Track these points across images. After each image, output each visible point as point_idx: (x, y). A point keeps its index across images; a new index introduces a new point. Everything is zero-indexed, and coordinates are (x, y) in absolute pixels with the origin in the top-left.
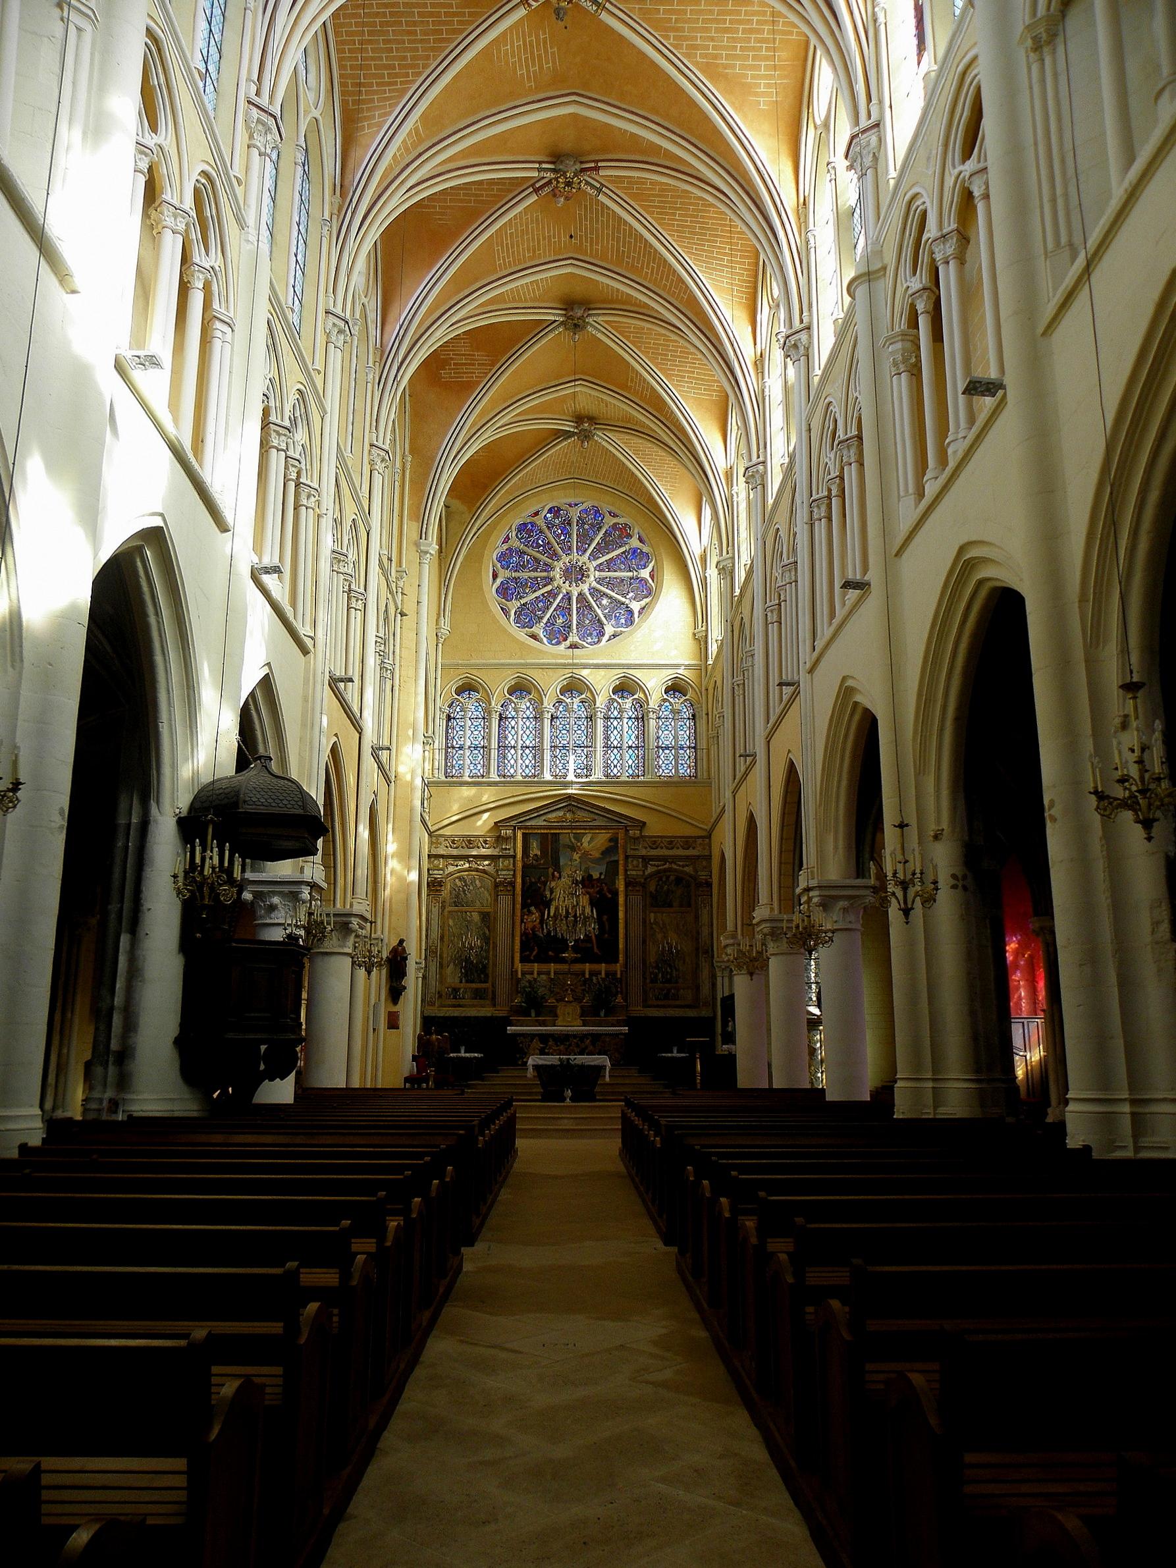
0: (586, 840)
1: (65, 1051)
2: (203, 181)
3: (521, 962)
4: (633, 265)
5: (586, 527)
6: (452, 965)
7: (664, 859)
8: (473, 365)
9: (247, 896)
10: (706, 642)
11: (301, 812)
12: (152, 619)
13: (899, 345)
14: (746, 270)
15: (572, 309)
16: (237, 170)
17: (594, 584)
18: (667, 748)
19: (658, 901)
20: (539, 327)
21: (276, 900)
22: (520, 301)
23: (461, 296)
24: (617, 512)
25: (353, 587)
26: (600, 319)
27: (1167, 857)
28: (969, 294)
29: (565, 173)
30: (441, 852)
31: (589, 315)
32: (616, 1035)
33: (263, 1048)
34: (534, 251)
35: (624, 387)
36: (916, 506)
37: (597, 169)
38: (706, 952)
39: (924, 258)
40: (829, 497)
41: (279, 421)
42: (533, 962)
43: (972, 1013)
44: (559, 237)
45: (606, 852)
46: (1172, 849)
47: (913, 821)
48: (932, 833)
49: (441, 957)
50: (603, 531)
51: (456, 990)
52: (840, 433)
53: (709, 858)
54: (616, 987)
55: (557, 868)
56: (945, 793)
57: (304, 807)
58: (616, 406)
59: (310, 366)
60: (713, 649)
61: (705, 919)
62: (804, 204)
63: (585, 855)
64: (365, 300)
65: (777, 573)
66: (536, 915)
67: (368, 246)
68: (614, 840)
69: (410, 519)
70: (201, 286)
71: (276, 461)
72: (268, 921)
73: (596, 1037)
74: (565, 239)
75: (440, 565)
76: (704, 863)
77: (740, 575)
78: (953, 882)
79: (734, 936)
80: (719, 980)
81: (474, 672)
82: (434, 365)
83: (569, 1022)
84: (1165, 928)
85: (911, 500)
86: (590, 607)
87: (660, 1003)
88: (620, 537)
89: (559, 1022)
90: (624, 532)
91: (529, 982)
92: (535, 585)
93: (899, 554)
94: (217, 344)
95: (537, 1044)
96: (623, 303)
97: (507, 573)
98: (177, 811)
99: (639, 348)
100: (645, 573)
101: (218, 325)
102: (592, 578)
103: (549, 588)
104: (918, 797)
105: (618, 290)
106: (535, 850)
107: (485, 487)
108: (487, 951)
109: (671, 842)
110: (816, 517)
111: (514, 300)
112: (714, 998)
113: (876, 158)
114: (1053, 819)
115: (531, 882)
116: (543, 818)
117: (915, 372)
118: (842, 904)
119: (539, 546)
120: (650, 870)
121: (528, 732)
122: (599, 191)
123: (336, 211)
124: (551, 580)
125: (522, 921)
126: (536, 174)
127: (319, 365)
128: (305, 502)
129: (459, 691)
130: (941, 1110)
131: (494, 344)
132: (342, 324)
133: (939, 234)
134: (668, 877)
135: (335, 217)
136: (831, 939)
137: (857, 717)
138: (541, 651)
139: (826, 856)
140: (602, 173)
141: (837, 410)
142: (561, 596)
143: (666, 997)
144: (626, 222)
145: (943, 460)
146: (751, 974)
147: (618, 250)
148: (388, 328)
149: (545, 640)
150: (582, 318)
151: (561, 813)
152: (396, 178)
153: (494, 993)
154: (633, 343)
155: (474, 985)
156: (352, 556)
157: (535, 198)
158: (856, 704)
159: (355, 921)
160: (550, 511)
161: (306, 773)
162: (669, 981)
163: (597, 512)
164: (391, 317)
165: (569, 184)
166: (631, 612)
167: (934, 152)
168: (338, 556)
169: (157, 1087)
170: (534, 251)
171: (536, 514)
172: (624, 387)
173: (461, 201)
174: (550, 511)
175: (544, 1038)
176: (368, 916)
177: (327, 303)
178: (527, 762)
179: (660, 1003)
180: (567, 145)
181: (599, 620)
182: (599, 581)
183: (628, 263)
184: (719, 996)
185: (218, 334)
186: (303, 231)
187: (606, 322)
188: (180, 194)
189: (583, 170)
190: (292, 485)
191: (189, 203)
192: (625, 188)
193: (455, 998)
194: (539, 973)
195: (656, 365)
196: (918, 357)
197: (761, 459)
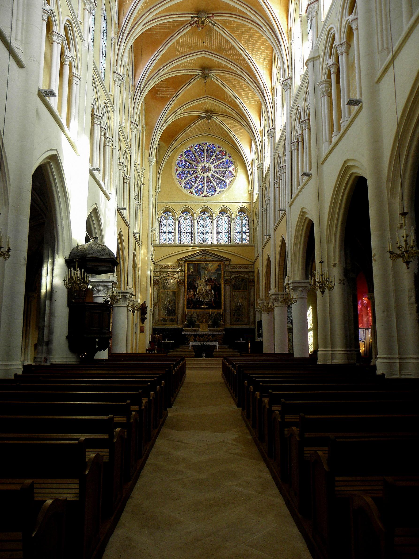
0: (210, 266)
1: (27, 340)
2: (68, 23)
3: (187, 309)
4: (227, 53)
5: (210, 152)
6: (162, 310)
7: (238, 273)
8: (168, 91)
9: (90, 286)
10: (253, 194)
11: (108, 257)
12: (54, 188)
13: (324, 85)
14: (268, 55)
15: (204, 70)
16: (80, 19)
17: (213, 173)
18: (239, 233)
19: (235, 287)
20: (192, 77)
21: (100, 288)
22: (185, 67)
23: (163, 65)
24: (221, 146)
25: (125, 175)
26: (215, 74)
27: (415, 274)
28: (350, 66)
29: (201, 18)
30: (158, 270)
31: (210, 72)
32: (221, 334)
33: (97, 340)
34: (190, 48)
35: (224, 100)
36: (329, 146)
37: (213, 16)
38: (252, 305)
39: (334, 52)
40: (298, 142)
41: (97, 114)
42: (191, 309)
43: (345, 328)
44: (199, 43)
45: (217, 270)
46: (416, 271)
47: (326, 260)
48: (332, 265)
49: (159, 307)
50: (216, 154)
51: (164, 319)
52: (302, 118)
53: (254, 272)
54: (221, 318)
55: (199, 275)
56: (337, 250)
57: (110, 255)
58: (220, 106)
59: (108, 92)
60: (255, 197)
61: (252, 294)
62: (290, 30)
63: (210, 271)
64: (128, 67)
65: (279, 169)
66: (192, 293)
67: (129, 47)
68: (220, 265)
69: (145, 149)
70: (68, 64)
71: (97, 129)
72: (98, 295)
73: (213, 335)
74: (201, 43)
75: (157, 166)
76: (252, 274)
77: (265, 170)
78: (340, 282)
79: (262, 300)
80: (257, 315)
81: (169, 205)
82: (154, 92)
83: (204, 330)
84: (413, 299)
85: (327, 143)
86: (211, 181)
87: (236, 323)
88: (222, 155)
89: (200, 330)
90: (223, 154)
91: (190, 316)
92: (191, 173)
93: (322, 163)
94: (74, 86)
95: (193, 338)
96: (223, 68)
97: (181, 169)
98: (65, 257)
99: (229, 85)
101: (74, 78)
102: (212, 171)
103: (196, 174)
104: (328, 251)
105: (221, 63)
106: (192, 270)
107: (173, 137)
108: (175, 305)
109: (240, 267)
110: (293, 149)
111: (183, 67)
112: (255, 322)
113: (317, 13)
114: (375, 260)
115: (190, 281)
116: (195, 258)
117: (330, 95)
118: (301, 289)
119: (192, 159)
120: (233, 276)
121: (189, 227)
122: (214, 25)
123: (117, 34)
124: (196, 172)
125: (187, 295)
126: (190, 19)
127: (112, 93)
128: (107, 144)
129: (164, 212)
130: (334, 361)
131: (176, 83)
132: (120, 77)
133: (339, 43)
134: (239, 279)
135: (116, 36)
136: (296, 301)
137: (307, 222)
138: (193, 198)
139: (295, 272)
140: (215, 18)
141: (301, 109)
142: (200, 177)
143: (238, 321)
144: (224, 37)
145: (339, 129)
146: (268, 313)
147: (221, 47)
148: (136, 78)
149: (195, 193)
150: (208, 74)
151: (201, 256)
152: (139, 21)
153: (177, 319)
154: (227, 83)
155: (171, 317)
156: (125, 163)
157: (190, 28)
158: (306, 218)
159: (128, 295)
160: (196, 146)
161: (110, 243)
162: (239, 316)
163: (213, 146)
164: (138, 74)
165: (203, 22)
166: (226, 183)
167: (339, 11)
168: (120, 164)
169: (61, 353)
170: (190, 48)
171: (191, 147)
172: (224, 100)
173: (163, 29)
174: (196, 146)
175: (195, 335)
176: (133, 293)
177: (114, 69)
178: (189, 238)
179: (236, 323)
180: (202, 7)
181: (214, 186)
182: (215, 172)
183: (225, 53)
184: (257, 321)
185: (75, 82)
186: (105, 41)
187: (217, 75)
188: (59, 29)
189: (208, 17)
190: (103, 138)
191: (62, 32)
192: (224, 24)
193: (164, 322)
194: (193, 313)
195: (235, 91)
196: (331, 89)
197: (273, 127)
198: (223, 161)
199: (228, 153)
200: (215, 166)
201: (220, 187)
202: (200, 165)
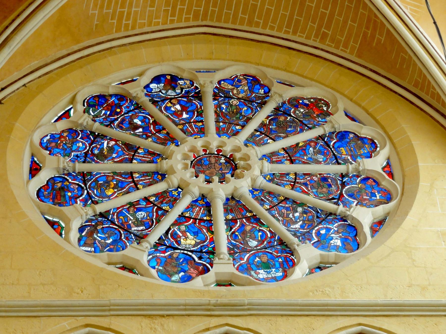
97: (64, 162)
100: (375, 164)
102: (257, 172)
103: (160, 187)
149: (154, 272)
160: (157, 79)
181: (281, 242)
198: (321, 137)
199: (341, 106)
200: (274, 154)
201: (322, 243)
202: (185, 148)
